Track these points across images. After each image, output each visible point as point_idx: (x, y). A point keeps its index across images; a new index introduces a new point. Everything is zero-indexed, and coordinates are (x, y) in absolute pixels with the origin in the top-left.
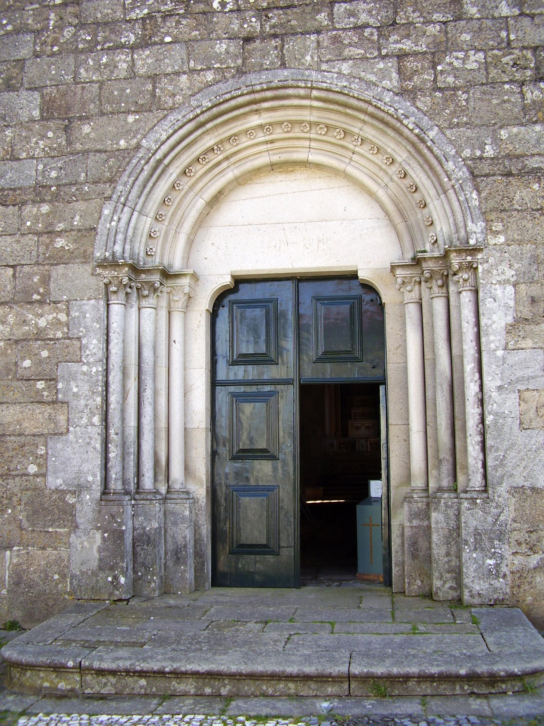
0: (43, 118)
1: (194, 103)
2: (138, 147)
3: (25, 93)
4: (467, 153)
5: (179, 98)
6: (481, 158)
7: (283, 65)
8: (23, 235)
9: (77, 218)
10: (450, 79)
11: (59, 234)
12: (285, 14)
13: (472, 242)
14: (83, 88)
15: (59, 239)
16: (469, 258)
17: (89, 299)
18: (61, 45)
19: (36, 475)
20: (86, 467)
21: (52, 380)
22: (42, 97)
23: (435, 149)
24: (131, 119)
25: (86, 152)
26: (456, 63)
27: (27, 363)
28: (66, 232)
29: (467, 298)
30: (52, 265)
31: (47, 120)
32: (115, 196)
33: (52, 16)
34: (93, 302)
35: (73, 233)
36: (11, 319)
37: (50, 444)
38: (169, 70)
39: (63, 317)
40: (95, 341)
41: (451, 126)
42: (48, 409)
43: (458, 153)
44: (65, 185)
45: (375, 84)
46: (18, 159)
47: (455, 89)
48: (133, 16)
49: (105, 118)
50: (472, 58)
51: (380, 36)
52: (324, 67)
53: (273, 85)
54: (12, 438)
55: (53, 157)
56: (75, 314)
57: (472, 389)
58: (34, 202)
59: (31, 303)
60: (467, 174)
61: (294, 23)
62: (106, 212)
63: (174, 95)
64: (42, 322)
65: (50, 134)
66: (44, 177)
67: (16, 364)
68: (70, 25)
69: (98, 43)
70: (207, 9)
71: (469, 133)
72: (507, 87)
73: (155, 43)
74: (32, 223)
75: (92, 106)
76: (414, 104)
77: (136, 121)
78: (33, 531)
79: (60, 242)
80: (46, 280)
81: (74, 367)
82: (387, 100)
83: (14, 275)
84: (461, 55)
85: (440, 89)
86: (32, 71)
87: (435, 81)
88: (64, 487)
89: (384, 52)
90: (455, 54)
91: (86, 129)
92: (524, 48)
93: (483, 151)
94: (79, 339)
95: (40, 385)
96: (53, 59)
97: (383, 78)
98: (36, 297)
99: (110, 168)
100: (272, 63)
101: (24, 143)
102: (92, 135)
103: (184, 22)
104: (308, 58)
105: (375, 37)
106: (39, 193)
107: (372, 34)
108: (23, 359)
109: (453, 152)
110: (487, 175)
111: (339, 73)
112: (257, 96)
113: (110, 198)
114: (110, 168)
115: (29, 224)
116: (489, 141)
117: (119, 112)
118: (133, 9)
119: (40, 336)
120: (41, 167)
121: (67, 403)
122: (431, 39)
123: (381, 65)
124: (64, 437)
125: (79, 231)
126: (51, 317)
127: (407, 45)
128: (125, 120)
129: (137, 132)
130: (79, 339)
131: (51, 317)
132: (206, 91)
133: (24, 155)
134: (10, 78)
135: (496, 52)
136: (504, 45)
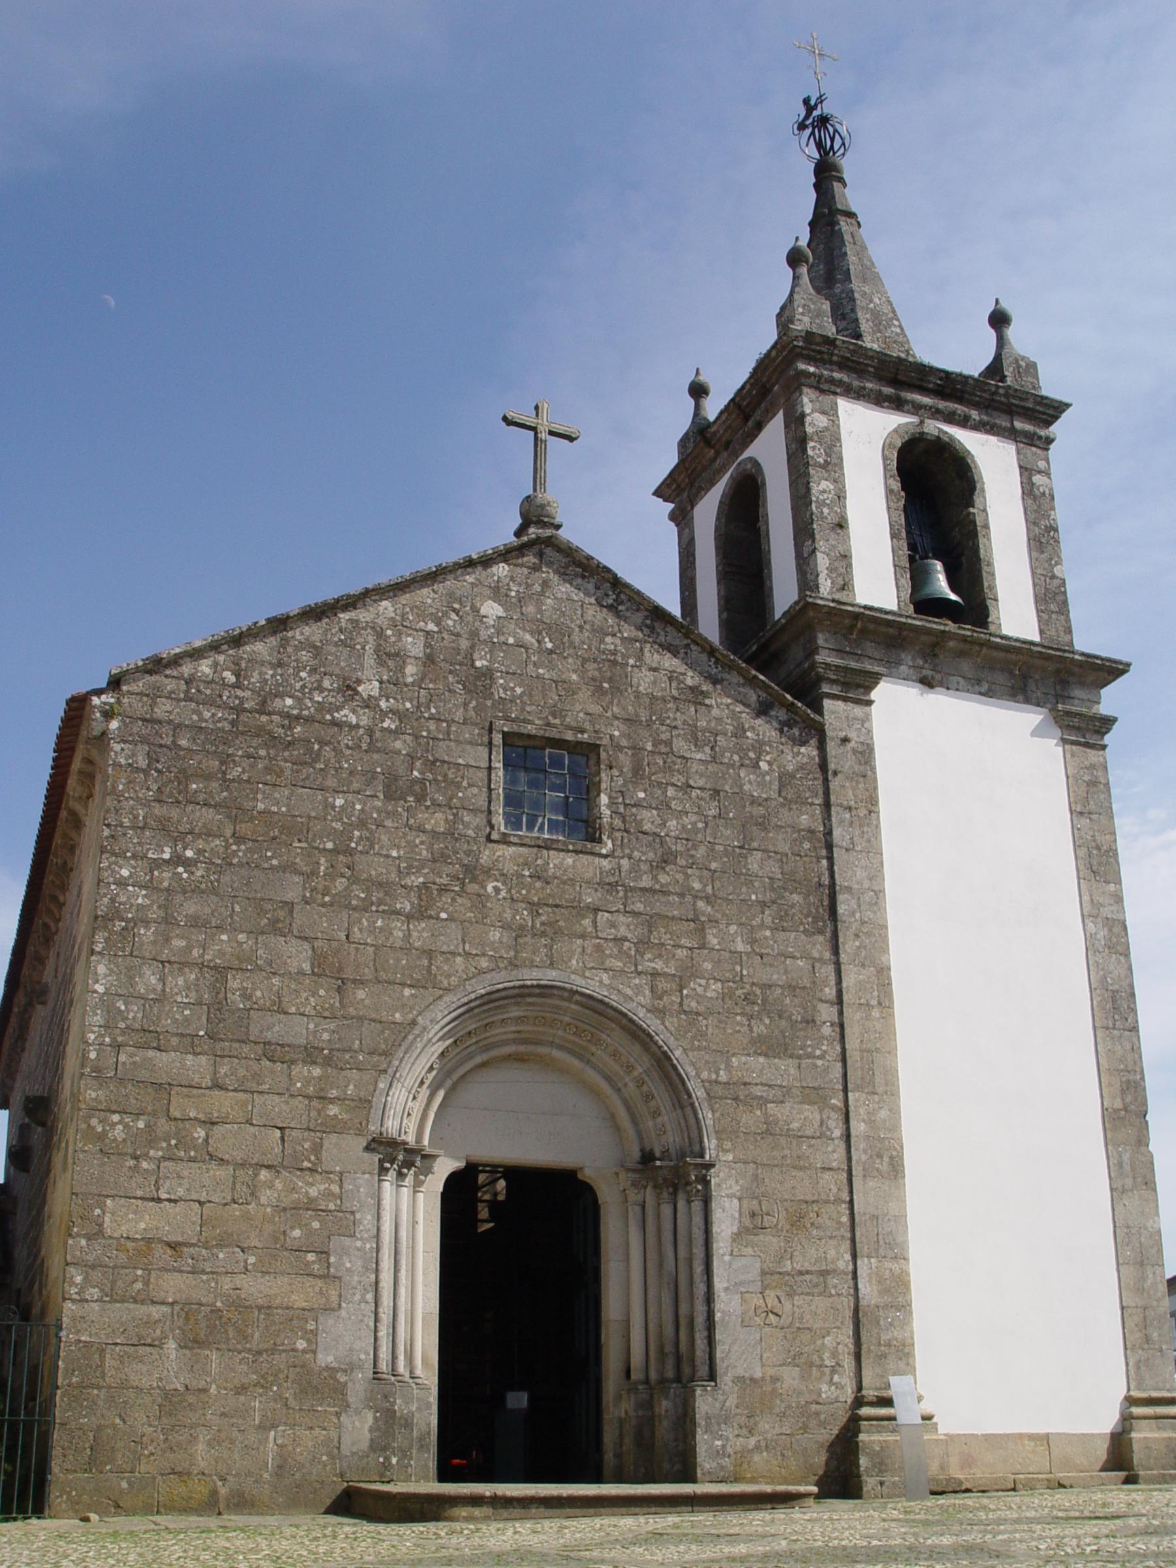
1: (469, 989)
2: (414, 1023)
3: (294, 941)
4: (705, 1075)
6: (716, 1082)
7: (552, 965)
9: (351, 1087)
10: (694, 1004)
11: (332, 1101)
12: (554, 913)
14: (357, 949)
15: (331, 1106)
16: (704, 1172)
17: (364, 1173)
19: (304, 1351)
20: (358, 1345)
21: (324, 1253)
24: (407, 992)
25: (360, 1019)
26: (699, 990)
27: (297, 1233)
28: (339, 1099)
29: (697, 1206)
30: (324, 1132)
31: (319, 976)
32: (390, 1070)
33: (323, 860)
34: (367, 1176)
36: (278, 1184)
37: (321, 1319)
38: (445, 948)
39: (335, 1188)
40: (369, 1217)
42: (320, 1283)
43: (698, 1075)
46: (286, 1013)
47: (698, 1014)
48: (408, 881)
49: (380, 986)
54: (279, 1311)
55: (325, 1018)
56: (348, 1186)
59: (301, 1170)
61: (561, 923)
62: (381, 1085)
63: (449, 976)
64: (313, 1192)
65: (322, 992)
66: (315, 1037)
69: (372, 904)
70: (482, 892)
71: (707, 1057)
72: (739, 1018)
73: (430, 917)
74: (303, 1085)
75: (367, 971)
76: (663, 1024)
77: (412, 995)
78: (301, 1409)
79: (333, 1110)
80: (317, 1148)
81: (347, 1241)
82: (641, 1015)
84: (703, 982)
86: (300, 918)
87: (681, 1004)
88: (335, 1365)
89: (640, 968)
90: (698, 980)
91: (361, 994)
93: (718, 1074)
94: (353, 1213)
95: (311, 1257)
98: (306, 1164)
100: (541, 961)
101: (294, 996)
102: (367, 1002)
103: (459, 900)
104: (574, 962)
105: (633, 953)
106: (311, 1054)
107: (630, 949)
108: (293, 1228)
109: (694, 1073)
110: (721, 1098)
111: (601, 982)
112: (526, 991)
113: (385, 1071)
114: (385, 1040)
115: (299, 1085)
116: (723, 1066)
119: (311, 1205)
120: (311, 1026)
121: (339, 1278)
122: (679, 963)
126: (322, 1187)
127: (659, 965)
129: (412, 1008)
130: (353, 1213)
131: (322, 1187)
132: (480, 978)
135: (731, 984)
136: (738, 979)
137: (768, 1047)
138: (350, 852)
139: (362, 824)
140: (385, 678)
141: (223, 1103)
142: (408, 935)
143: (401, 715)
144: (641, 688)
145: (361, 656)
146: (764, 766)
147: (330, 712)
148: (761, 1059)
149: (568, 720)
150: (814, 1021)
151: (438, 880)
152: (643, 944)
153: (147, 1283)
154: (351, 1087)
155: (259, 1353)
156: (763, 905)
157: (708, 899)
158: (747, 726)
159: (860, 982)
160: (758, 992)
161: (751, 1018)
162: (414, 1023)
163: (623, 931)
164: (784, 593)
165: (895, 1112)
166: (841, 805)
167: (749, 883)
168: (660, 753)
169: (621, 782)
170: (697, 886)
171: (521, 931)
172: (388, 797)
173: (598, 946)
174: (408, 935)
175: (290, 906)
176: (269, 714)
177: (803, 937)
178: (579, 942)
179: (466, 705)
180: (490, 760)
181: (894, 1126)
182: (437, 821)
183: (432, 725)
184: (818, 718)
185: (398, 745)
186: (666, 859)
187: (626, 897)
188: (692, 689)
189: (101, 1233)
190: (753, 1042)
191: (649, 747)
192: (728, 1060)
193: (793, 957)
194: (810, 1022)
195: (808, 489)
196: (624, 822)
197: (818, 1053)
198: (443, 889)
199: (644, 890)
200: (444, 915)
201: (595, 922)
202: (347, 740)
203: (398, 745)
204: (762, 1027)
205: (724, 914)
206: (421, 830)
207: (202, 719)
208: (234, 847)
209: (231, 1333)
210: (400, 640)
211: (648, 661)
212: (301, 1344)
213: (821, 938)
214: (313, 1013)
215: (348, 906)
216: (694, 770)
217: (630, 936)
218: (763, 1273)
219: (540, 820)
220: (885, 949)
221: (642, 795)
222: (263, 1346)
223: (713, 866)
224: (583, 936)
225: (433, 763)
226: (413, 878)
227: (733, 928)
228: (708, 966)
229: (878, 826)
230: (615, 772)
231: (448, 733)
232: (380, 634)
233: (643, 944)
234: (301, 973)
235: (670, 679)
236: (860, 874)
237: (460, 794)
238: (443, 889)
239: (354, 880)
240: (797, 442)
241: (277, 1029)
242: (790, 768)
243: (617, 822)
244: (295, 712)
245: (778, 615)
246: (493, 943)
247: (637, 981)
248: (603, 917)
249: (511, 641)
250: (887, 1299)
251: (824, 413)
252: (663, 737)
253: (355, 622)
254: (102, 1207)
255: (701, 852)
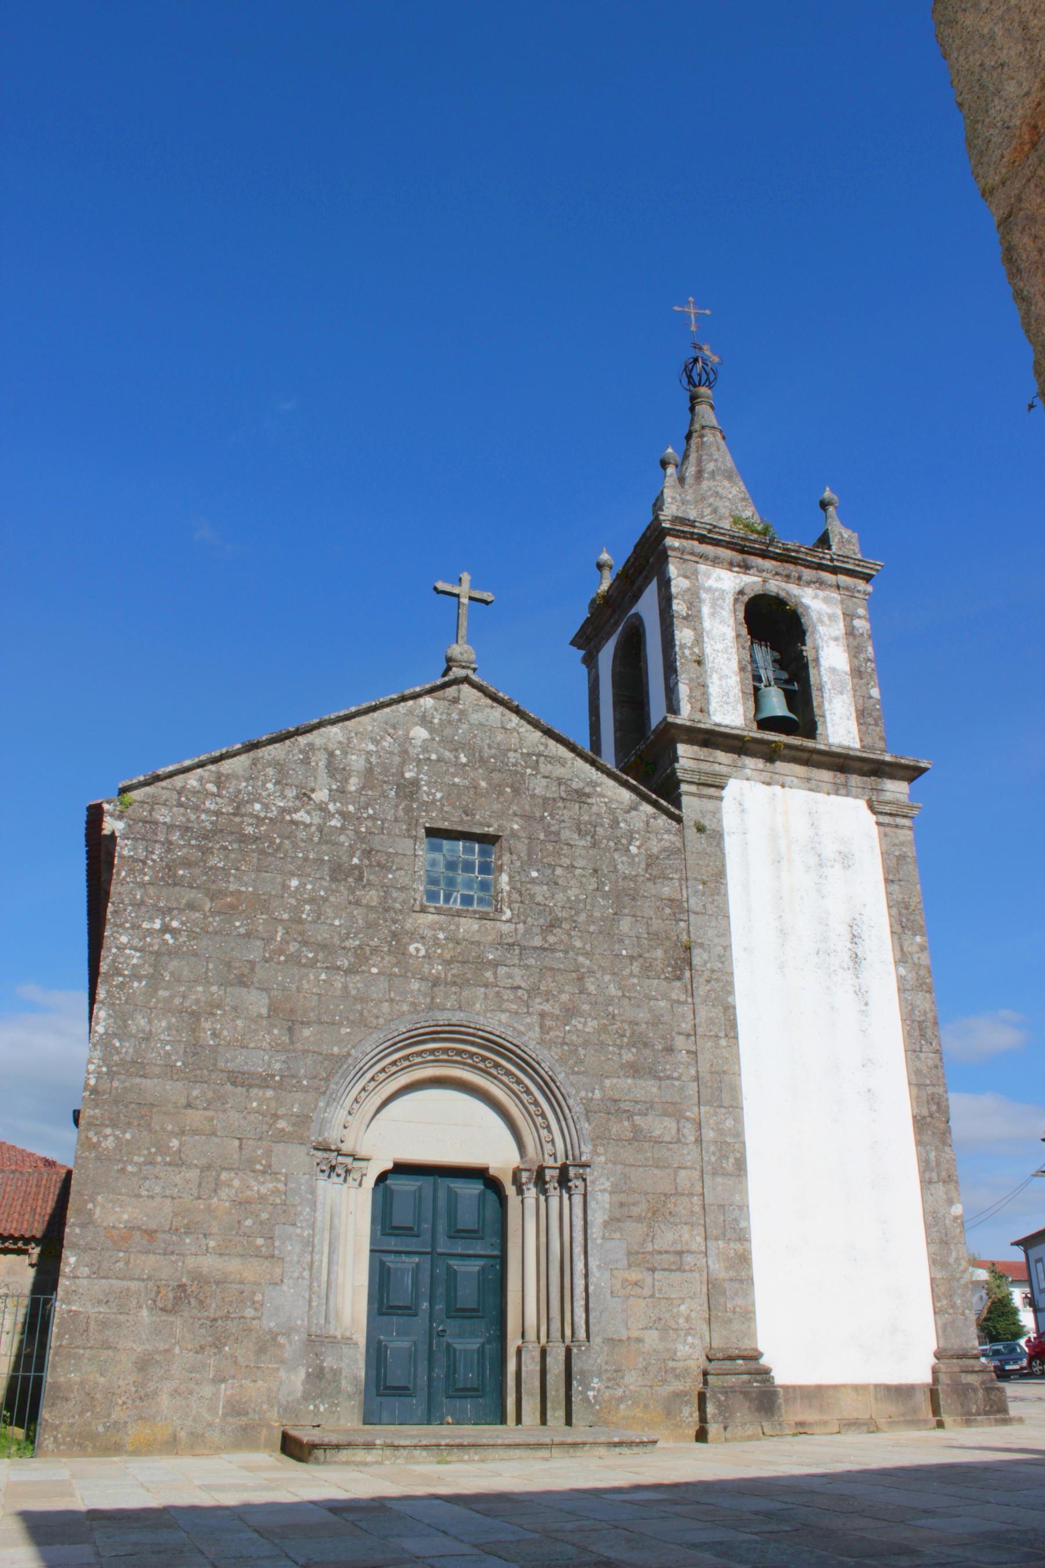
0: (269, 1016)
1: (393, 1027)
3: (254, 991)
4: (583, 1094)
5: (381, 1021)
6: (592, 1099)
8: (249, 1113)
9: (297, 1105)
10: (574, 1038)
13: (584, 1159)
16: (581, 1171)
18: (287, 956)
22: (269, 997)
23: (562, 1089)
25: (305, 1052)
26: (580, 1027)
27: (249, 1222)
33: (280, 929)
34: (307, 1176)
35: (293, 1118)
36: (236, 1183)
39: (281, 1186)
41: (574, 1073)
44: (287, 1076)
45: (523, 1034)
50: (589, 1024)
51: (529, 997)
52: (489, 1015)
53: (451, 1022)
57: (579, 1266)
58: (260, 1087)
59: (253, 1171)
60: (583, 1110)
62: (321, 1104)
63: (377, 1017)
64: (263, 1190)
67: (239, 1222)
68: (295, 940)
71: (585, 1079)
73: (363, 972)
75: (312, 1014)
80: (268, 1153)
81: (290, 1229)
82: (531, 1047)
83: (240, 1147)
84: (583, 1020)
85: (567, 1044)
86: (260, 973)
87: (564, 1038)
90: (579, 1019)
91: (307, 1032)
92: (622, 1022)
96: (280, 967)
97: (530, 1030)
98: (259, 1167)
99: (325, 1068)
100: (452, 1005)
104: (478, 1005)
105: (525, 997)
106: (264, 1081)
108: (246, 1218)
110: (595, 1112)
111: (500, 1021)
116: (597, 1087)
117: (333, 1024)
118: (347, 938)
120: (266, 1058)
121: (282, 1259)
123: (528, 1020)
124: (278, 1287)
125: (298, 1116)
126: (271, 1186)
127: (547, 1007)
128: (339, 1031)
133: (252, 1045)
134: (243, 975)
137: (634, 1070)
138: (300, 921)
139: (312, 901)
140: (334, 787)
141: (195, 1118)
142: (345, 987)
143: (344, 815)
144: (536, 791)
145: (315, 769)
146: (633, 849)
147: (290, 813)
148: (629, 1081)
149: (477, 817)
150: (672, 1050)
151: (371, 943)
152: (533, 991)
153: (127, 1263)
154: (297, 1105)
155: (215, 1320)
156: (632, 958)
157: (586, 954)
158: (620, 819)
159: (710, 1018)
160: (627, 1027)
161: (621, 1047)
162: (349, 1055)
163: (518, 981)
164: (657, 713)
165: (739, 1120)
166: (696, 879)
167: (622, 941)
168: (550, 841)
169: (518, 864)
170: (578, 944)
171: (436, 982)
172: (333, 879)
173: (498, 993)
174: (345, 987)
175: (253, 963)
176: (242, 816)
177: (664, 983)
178: (483, 990)
179: (397, 806)
180: (415, 850)
181: (738, 1134)
182: (372, 896)
183: (369, 823)
184: (677, 812)
185: (342, 838)
186: (553, 925)
187: (521, 954)
188: (577, 791)
189: (91, 1222)
190: (622, 1066)
191: (542, 836)
192: (601, 1084)
193: (656, 999)
194: (670, 1050)
195: (673, 635)
196: (521, 895)
197: (676, 1075)
198: (375, 950)
199: (535, 948)
200: (374, 970)
201: (495, 974)
202: (302, 835)
203: (342, 838)
204: (630, 1055)
205: (600, 966)
206: (357, 903)
207: (188, 820)
208: (211, 919)
209: (193, 1301)
210: (346, 758)
211: (542, 770)
212: (249, 1312)
213: (678, 984)
214: (268, 1047)
215: (299, 963)
216: (577, 854)
217: (523, 985)
218: (629, 1253)
219: (455, 894)
220: (731, 992)
221: (534, 874)
222: (218, 1314)
223: (592, 928)
224: (486, 986)
225: (370, 852)
226: (351, 941)
227: (607, 978)
228: (586, 1007)
229: (726, 895)
230: (515, 857)
231: (382, 829)
232: (331, 754)
233: (533, 991)
234: (260, 1016)
235: (560, 784)
236: (711, 933)
237: (390, 876)
238: (375, 950)
239: (305, 943)
240: (666, 599)
241: (239, 1061)
242: (655, 850)
243: (515, 896)
244: (262, 815)
245: (653, 727)
246: (413, 991)
247: (528, 1020)
248: (502, 970)
249: (434, 757)
250: (732, 1274)
251: (686, 577)
252: (553, 829)
253: (311, 746)
254: (93, 1200)
255: (582, 917)
